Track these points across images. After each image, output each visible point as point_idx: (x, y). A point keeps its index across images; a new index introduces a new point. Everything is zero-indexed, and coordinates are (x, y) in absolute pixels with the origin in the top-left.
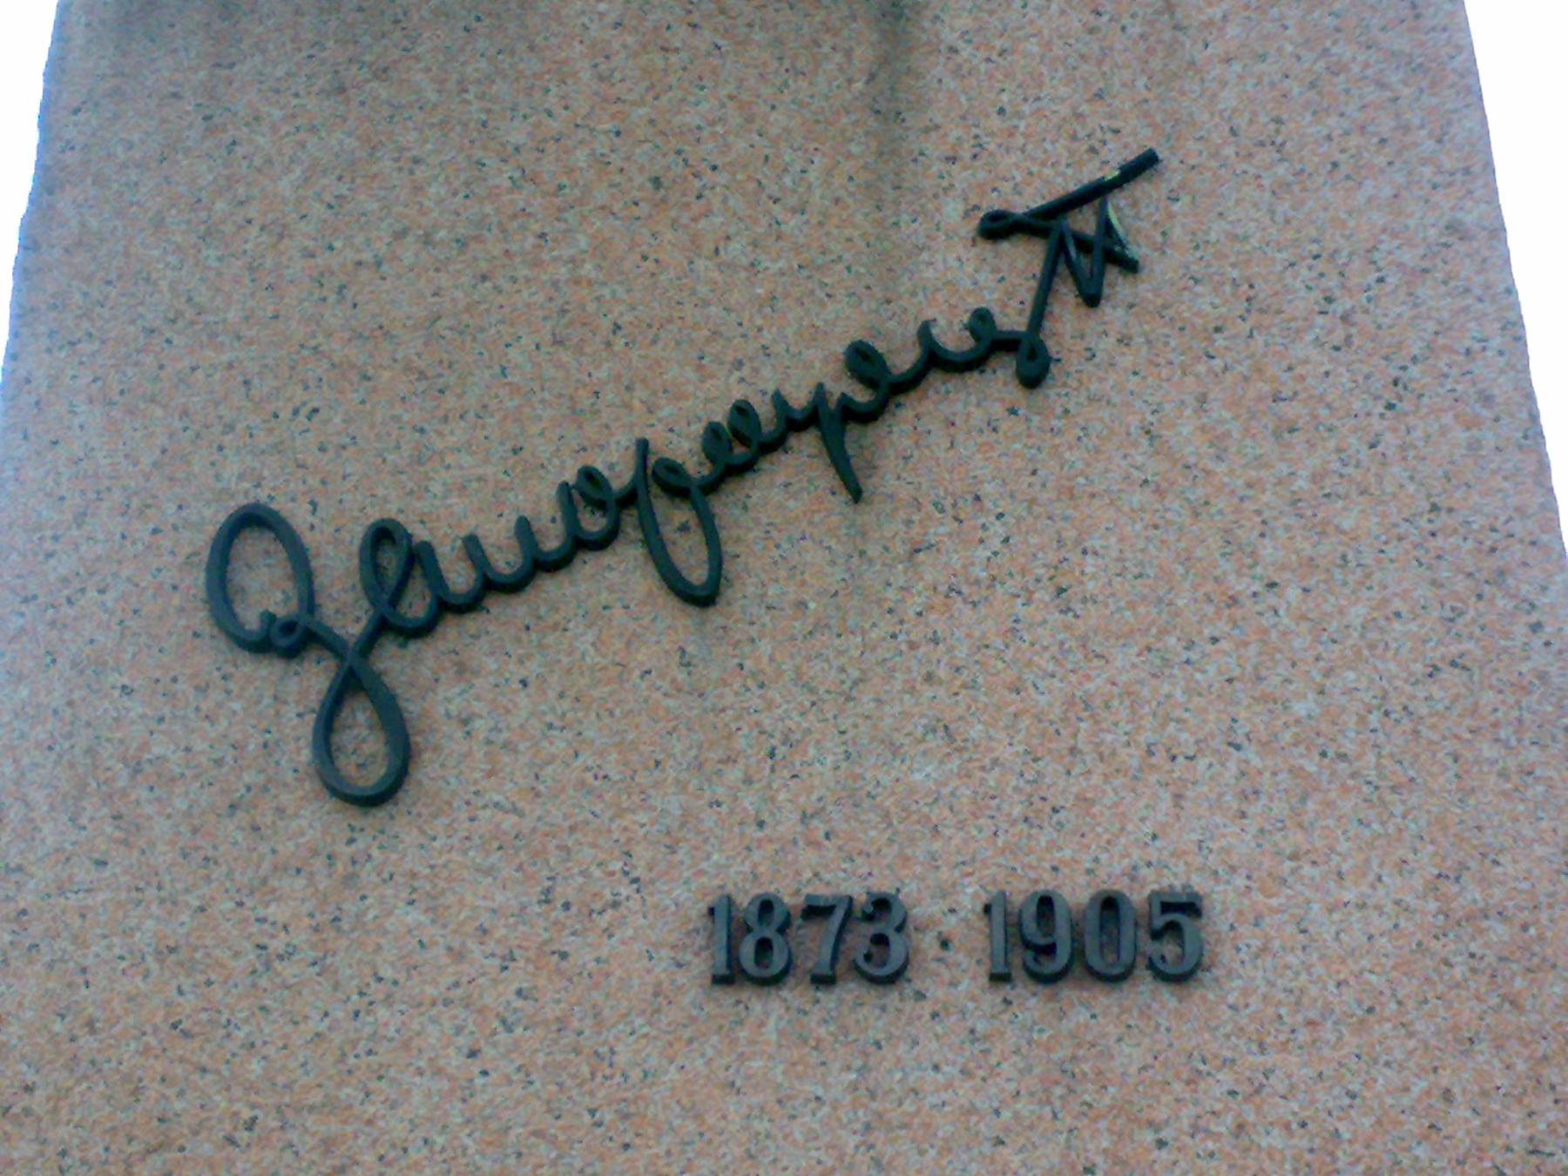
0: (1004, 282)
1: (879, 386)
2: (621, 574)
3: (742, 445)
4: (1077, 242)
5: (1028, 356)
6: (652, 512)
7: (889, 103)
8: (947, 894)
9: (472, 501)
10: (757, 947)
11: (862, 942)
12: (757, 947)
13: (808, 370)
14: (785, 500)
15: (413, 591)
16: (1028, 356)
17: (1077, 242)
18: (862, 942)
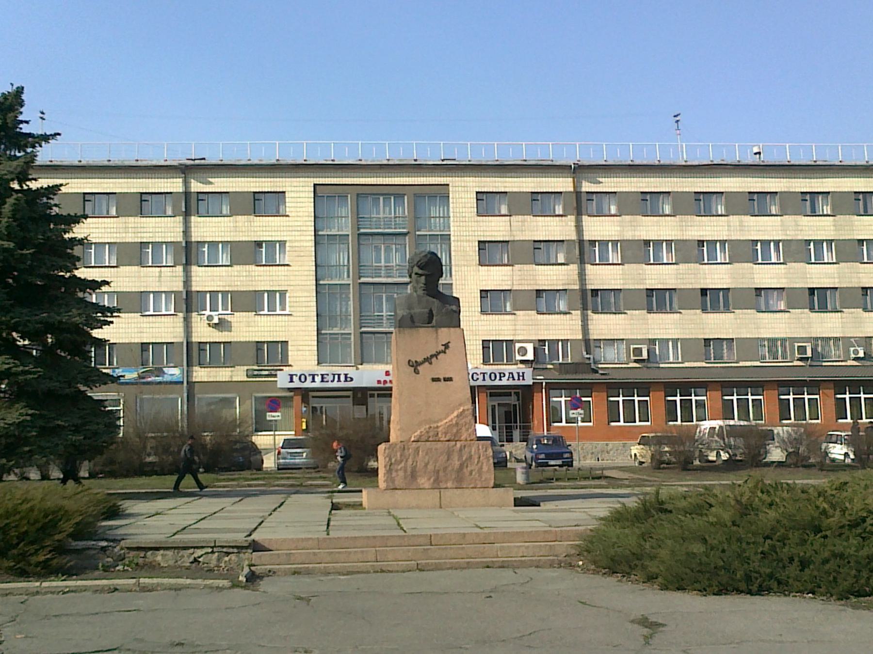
0: (443, 348)
1: (439, 353)
2: (427, 363)
3: (432, 356)
4: (446, 346)
5: (445, 352)
6: (428, 360)
7: (437, 342)
8: (442, 378)
9: (419, 360)
10: (434, 380)
11: (438, 380)
12: (434, 380)
13: (434, 353)
14: (434, 360)
15: (418, 364)
16: (445, 352)
17: (446, 346)
18: (438, 380)
